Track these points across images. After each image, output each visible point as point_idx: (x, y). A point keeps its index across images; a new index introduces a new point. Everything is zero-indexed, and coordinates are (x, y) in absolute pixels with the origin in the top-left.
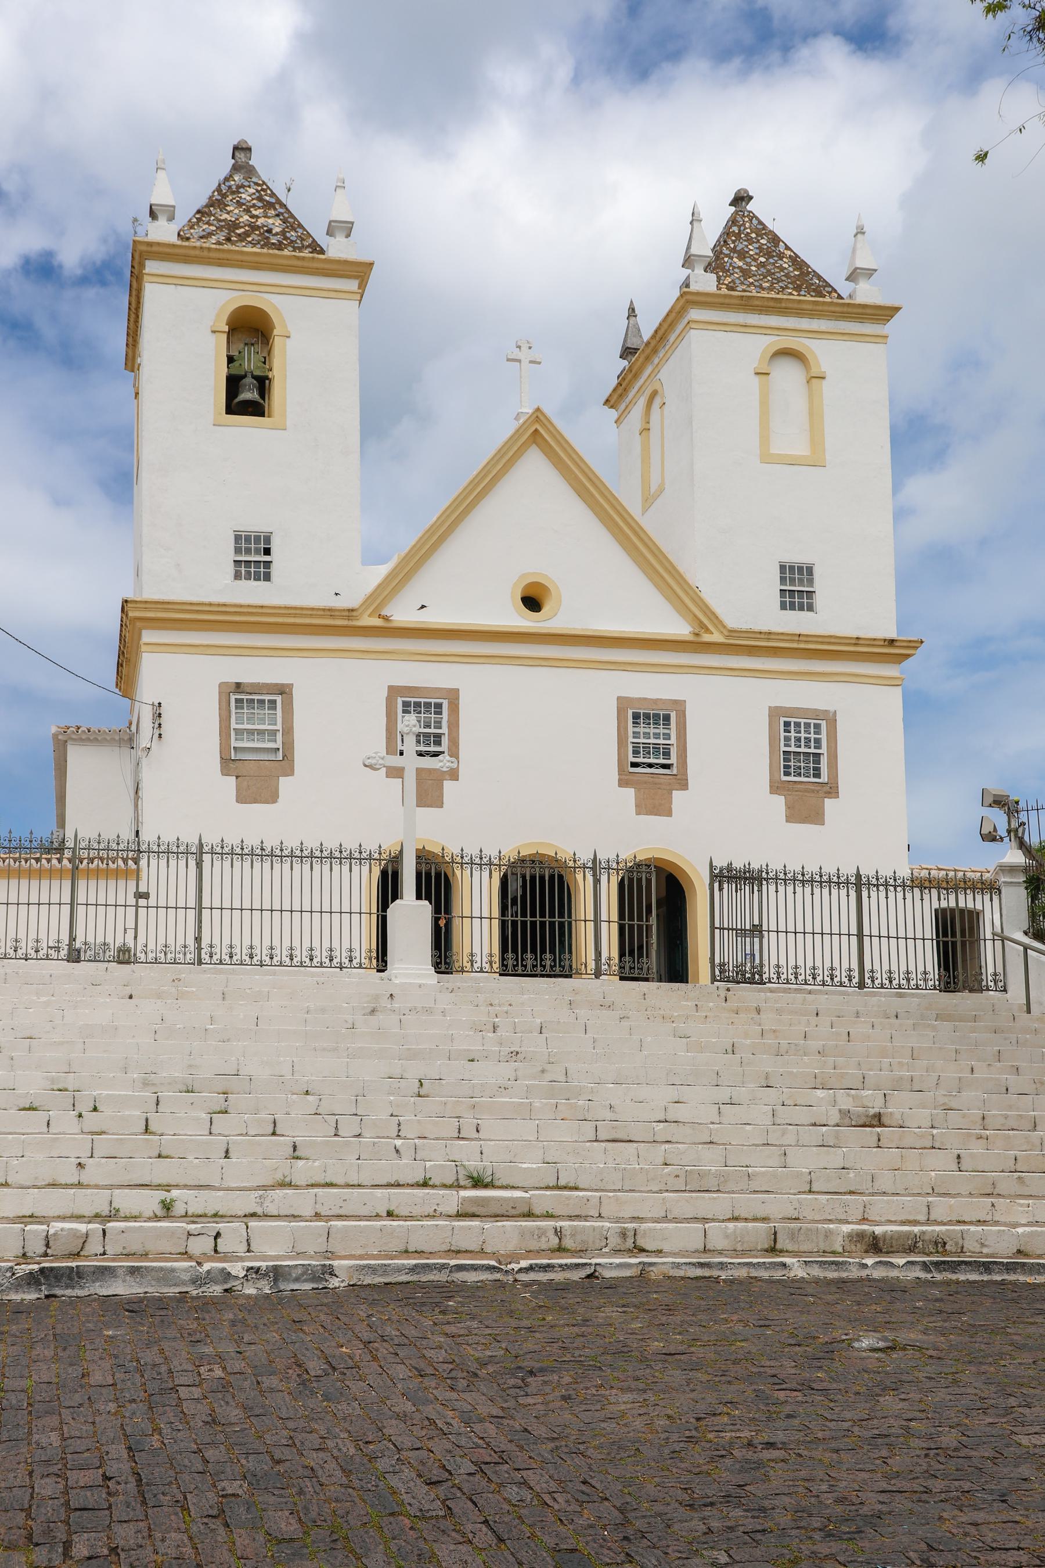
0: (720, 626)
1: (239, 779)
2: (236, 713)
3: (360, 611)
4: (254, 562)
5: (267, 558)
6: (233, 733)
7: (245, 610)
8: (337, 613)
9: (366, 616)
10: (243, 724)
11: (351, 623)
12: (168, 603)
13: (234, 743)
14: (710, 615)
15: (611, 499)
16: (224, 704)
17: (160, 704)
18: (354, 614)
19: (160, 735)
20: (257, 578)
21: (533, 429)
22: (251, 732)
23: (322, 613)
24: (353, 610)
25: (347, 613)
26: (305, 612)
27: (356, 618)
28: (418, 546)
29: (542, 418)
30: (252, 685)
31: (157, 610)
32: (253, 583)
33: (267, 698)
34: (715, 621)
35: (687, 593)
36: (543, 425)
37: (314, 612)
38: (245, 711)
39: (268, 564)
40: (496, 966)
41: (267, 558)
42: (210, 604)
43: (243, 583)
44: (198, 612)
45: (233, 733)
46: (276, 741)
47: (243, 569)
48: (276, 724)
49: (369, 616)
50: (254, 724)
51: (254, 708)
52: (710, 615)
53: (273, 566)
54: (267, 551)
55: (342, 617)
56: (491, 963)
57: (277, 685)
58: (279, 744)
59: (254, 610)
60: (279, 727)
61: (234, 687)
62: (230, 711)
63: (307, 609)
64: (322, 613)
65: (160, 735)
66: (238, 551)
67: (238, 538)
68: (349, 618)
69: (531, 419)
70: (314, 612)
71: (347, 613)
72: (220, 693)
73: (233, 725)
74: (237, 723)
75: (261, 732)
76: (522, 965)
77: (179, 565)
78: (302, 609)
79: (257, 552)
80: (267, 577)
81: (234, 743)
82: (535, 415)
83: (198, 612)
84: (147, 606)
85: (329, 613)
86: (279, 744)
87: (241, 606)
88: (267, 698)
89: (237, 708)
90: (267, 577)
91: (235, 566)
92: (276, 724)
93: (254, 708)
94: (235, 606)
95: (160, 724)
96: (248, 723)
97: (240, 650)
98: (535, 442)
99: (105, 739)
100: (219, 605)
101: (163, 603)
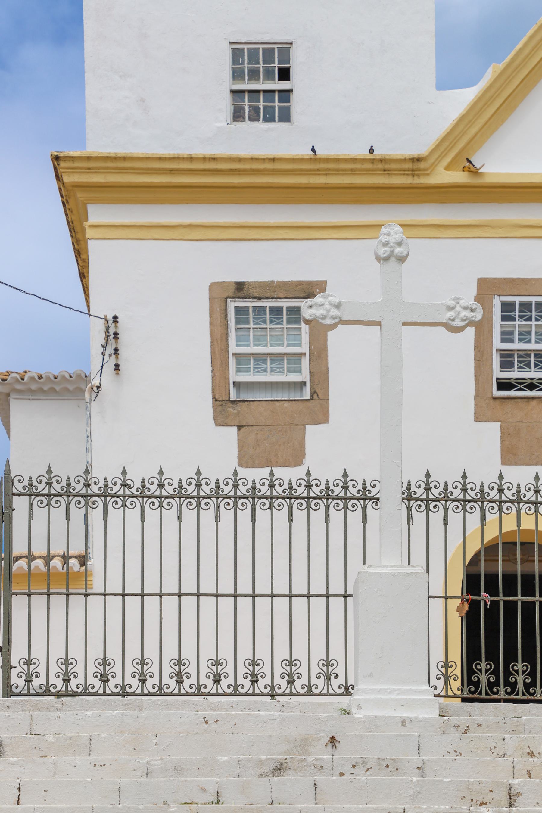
1: (243, 430)
2: (237, 329)
4: (265, 91)
5: (284, 85)
6: (232, 362)
7: (247, 166)
8: (393, 166)
9: (441, 168)
10: (248, 345)
11: (417, 181)
12: (124, 159)
13: (234, 376)
16: (218, 316)
17: (115, 318)
18: (422, 165)
19: (117, 366)
20: (269, 118)
22: (260, 358)
23: (369, 166)
24: (419, 160)
25: (409, 165)
26: (342, 166)
27: (426, 173)
28: (527, 51)
30: (263, 285)
31: (106, 170)
32: (261, 126)
33: (285, 304)
37: (358, 166)
38: (252, 325)
39: (285, 94)
40: (456, 685)
41: (284, 85)
42: (191, 159)
43: (247, 126)
44: (172, 171)
45: (232, 362)
46: (300, 371)
47: (246, 105)
48: (300, 345)
49: (447, 168)
50: (266, 346)
51: (265, 322)
53: (294, 97)
54: (285, 74)
55: (403, 172)
56: (447, 678)
57: (300, 283)
58: (305, 376)
59: (261, 166)
60: (305, 348)
61: (233, 288)
62: (227, 327)
63: (346, 161)
64: (369, 166)
65: (117, 366)
66: (237, 75)
67: (237, 54)
68: (414, 173)
70: (358, 166)
71: (409, 165)
72: (211, 299)
73: (233, 348)
74: (238, 345)
75: (277, 358)
76: (507, 683)
77: (143, 100)
78: (337, 160)
79: (269, 75)
80: (285, 117)
81: (234, 376)
83: (172, 171)
84: (92, 164)
85: (380, 166)
86: (305, 376)
87: (240, 160)
88: (285, 304)
89: (238, 322)
90: (285, 117)
91: (234, 100)
92: (300, 345)
93: (265, 322)
94: (231, 159)
95: (116, 350)
96: (255, 345)
97: (246, 231)
99: (67, 390)
100: (204, 159)
101: (116, 159)
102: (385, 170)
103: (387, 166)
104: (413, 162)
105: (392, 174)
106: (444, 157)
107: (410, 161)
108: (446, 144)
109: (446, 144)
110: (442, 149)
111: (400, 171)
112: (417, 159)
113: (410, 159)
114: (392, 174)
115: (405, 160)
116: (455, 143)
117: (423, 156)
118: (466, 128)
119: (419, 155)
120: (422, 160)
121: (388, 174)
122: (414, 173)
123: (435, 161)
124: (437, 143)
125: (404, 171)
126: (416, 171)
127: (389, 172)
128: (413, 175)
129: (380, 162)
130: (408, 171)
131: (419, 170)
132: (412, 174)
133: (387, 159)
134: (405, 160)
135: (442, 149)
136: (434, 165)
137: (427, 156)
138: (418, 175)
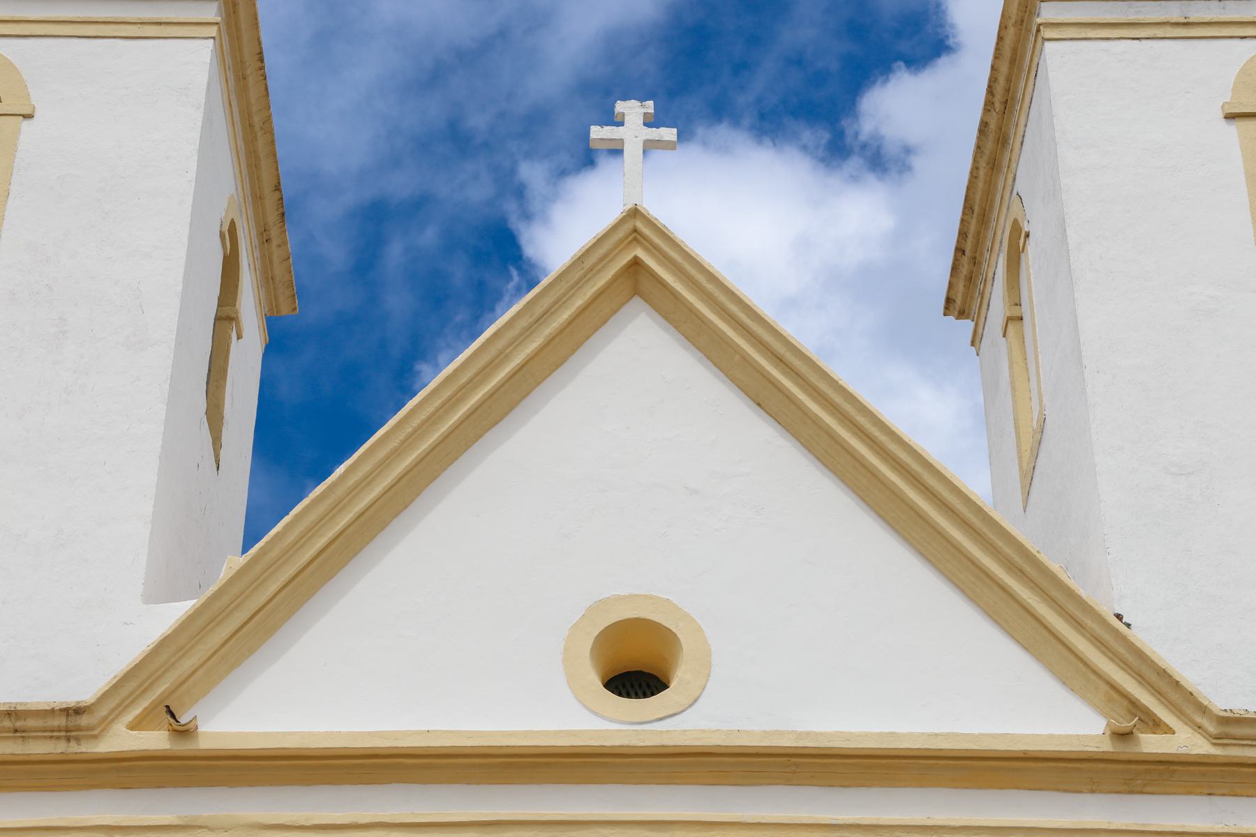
0: (1189, 711)
3: (103, 712)
8: (31, 723)
11: (74, 748)
14: (1153, 678)
15: (838, 399)
18: (84, 720)
21: (628, 257)
24: (78, 711)
29: (646, 231)
34: (1174, 696)
35: (1079, 626)
36: (653, 249)
52: (1153, 678)
55: (50, 734)
68: (69, 734)
69: (621, 234)
71: (60, 721)
82: (628, 227)
98: (636, 292)
102: (16, 731)
103: (19, 724)
104: (68, 715)
105: (29, 737)
106: (127, 706)
107: (62, 713)
108: (133, 684)
109: (133, 684)
110: (125, 692)
111: (44, 731)
112: (74, 710)
113: (62, 710)
114: (29, 737)
115: (52, 712)
116: (152, 684)
117: (85, 705)
118: (173, 660)
119: (78, 703)
120: (84, 712)
121: (23, 737)
122: (69, 734)
123: (110, 714)
124: (114, 682)
125: (52, 731)
126: (74, 731)
127: (24, 734)
128: (68, 739)
129: (7, 716)
130: (60, 731)
131: (79, 729)
132: (66, 736)
133: (19, 710)
134: (53, 711)
135: (125, 692)
136: (108, 721)
137: (92, 704)
138: (78, 739)
